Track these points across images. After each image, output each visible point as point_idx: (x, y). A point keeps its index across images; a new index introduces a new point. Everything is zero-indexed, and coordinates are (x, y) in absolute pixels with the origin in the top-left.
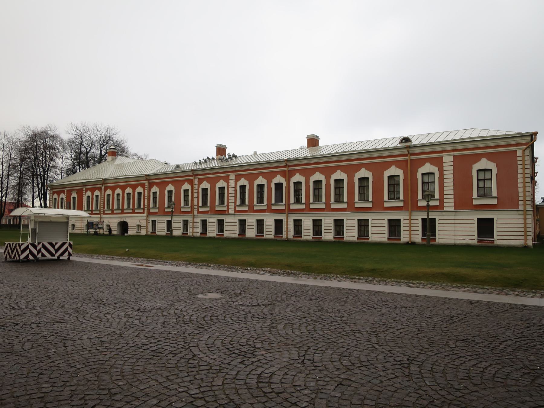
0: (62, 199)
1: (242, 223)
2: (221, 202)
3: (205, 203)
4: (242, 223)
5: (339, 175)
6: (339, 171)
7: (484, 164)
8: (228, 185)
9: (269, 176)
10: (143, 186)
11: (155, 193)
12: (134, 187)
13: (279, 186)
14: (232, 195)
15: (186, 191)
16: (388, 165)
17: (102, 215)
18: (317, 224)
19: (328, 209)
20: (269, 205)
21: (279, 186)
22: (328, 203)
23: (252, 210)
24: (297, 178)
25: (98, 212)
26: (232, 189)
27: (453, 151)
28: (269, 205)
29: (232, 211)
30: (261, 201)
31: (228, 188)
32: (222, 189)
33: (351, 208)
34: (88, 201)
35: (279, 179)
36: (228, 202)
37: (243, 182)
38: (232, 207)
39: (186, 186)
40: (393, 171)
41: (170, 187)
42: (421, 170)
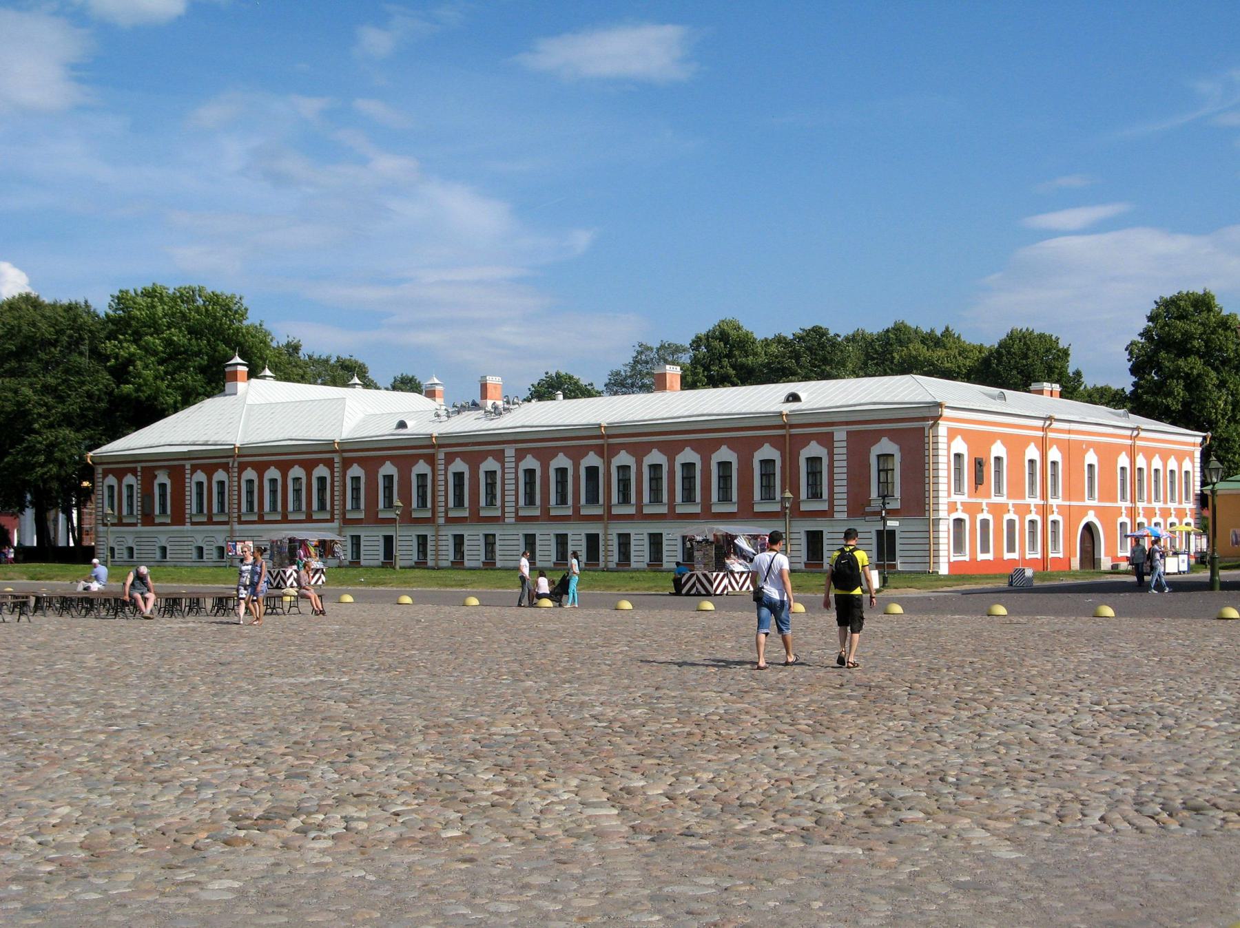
0: (130, 487)
3: (459, 502)
6: (688, 449)
8: (503, 468)
10: (329, 464)
11: (356, 480)
12: (309, 466)
13: (592, 472)
14: (510, 487)
15: (422, 477)
17: (237, 527)
21: (592, 472)
22: (672, 505)
23: (547, 517)
25: (225, 519)
26: (510, 476)
27: (847, 423)
29: (510, 519)
31: (503, 473)
32: (491, 474)
34: (200, 495)
35: (592, 459)
36: (503, 501)
37: (530, 462)
38: (510, 509)
41: (388, 469)
42: (806, 453)
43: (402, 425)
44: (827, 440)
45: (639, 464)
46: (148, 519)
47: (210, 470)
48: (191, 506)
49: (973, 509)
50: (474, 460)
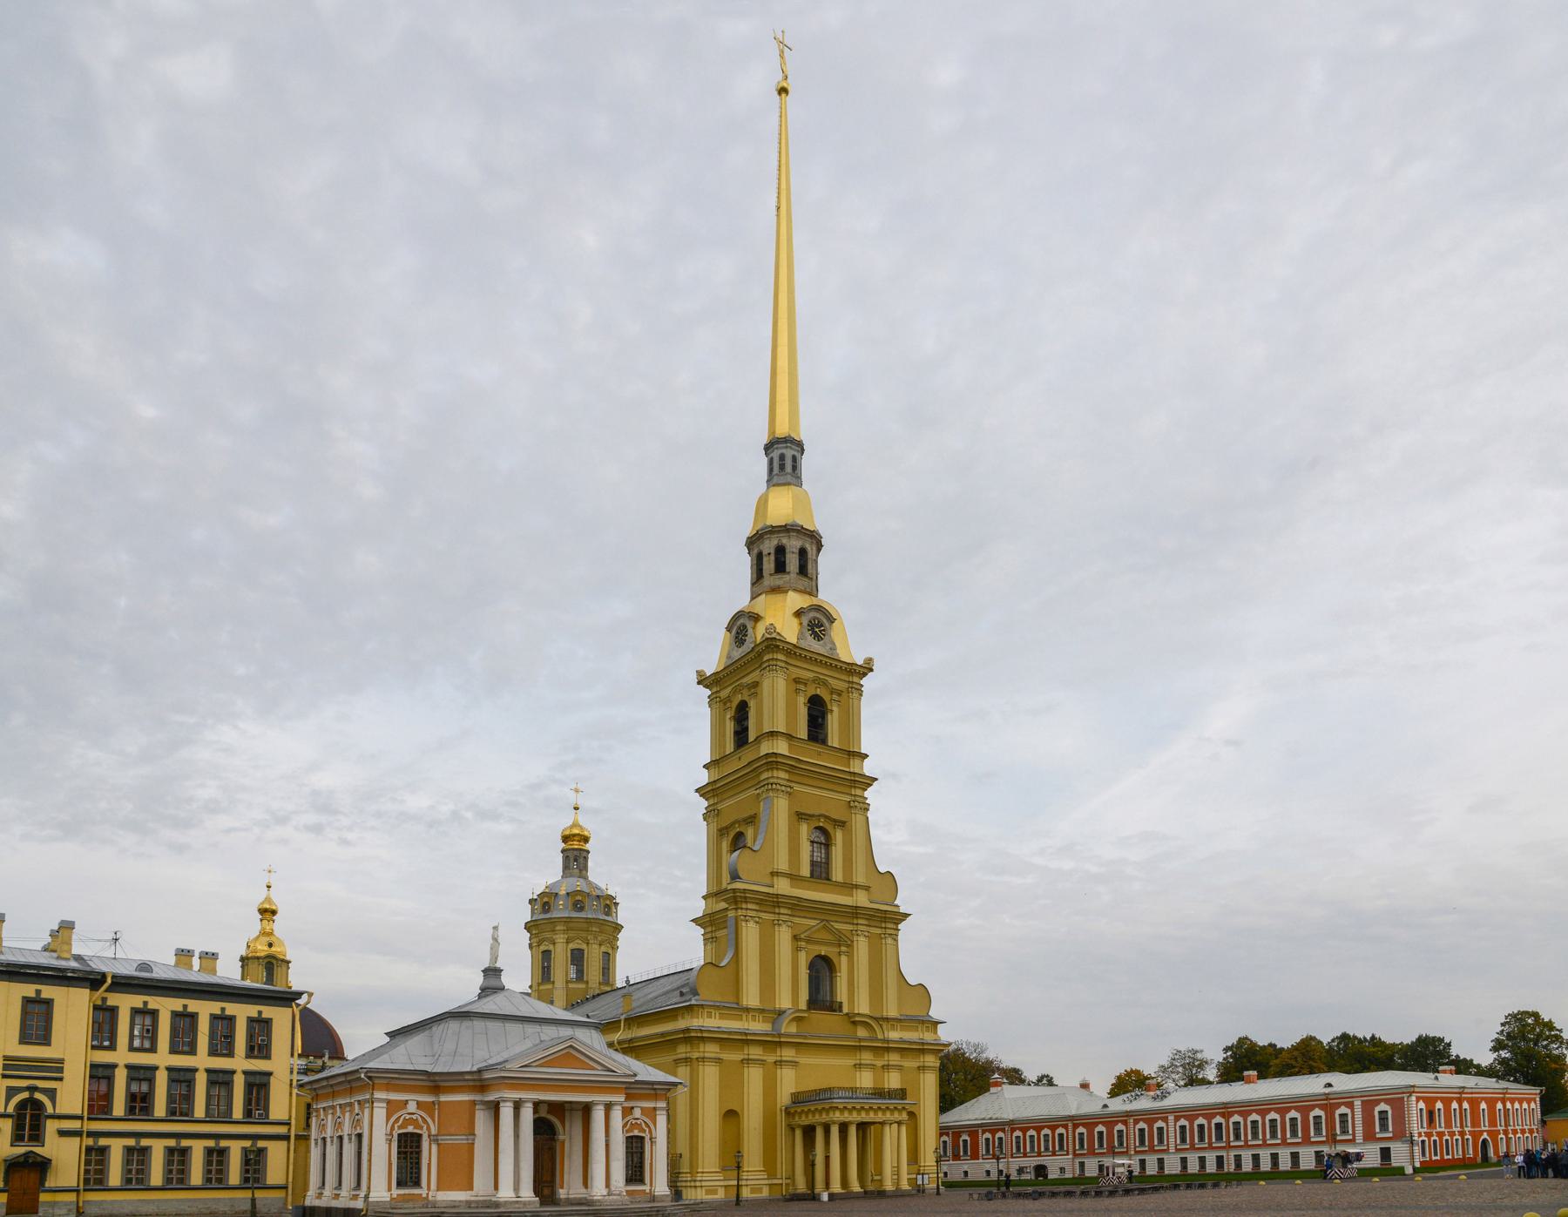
1: (1184, 1160)
2: (1161, 1141)
3: (1142, 1143)
4: (1184, 1160)
5: (1273, 1115)
7: (1383, 1107)
9: (1209, 1117)
10: (1066, 1127)
12: (1053, 1128)
14: (1172, 1134)
15: (1120, 1132)
16: (1313, 1107)
18: (1256, 1158)
19: (1265, 1145)
20: (1210, 1143)
21: (1219, 1126)
23: (1193, 1148)
24: (1236, 1118)
26: (1171, 1129)
28: (1210, 1143)
29: (1172, 1150)
30: (1202, 1139)
32: (1160, 1130)
33: (1284, 1143)
35: (1218, 1119)
37: (1183, 1122)
38: (1172, 1146)
39: (1120, 1127)
40: (1317, 1112)
41: (1101, 1128)
43: (1105, 1106)
44: (1350, 1105)
46: (956, 1157)
47: (993, 1132)
48: (982, 1150)
49: (1429, 1135)
50: (1150, 1122)
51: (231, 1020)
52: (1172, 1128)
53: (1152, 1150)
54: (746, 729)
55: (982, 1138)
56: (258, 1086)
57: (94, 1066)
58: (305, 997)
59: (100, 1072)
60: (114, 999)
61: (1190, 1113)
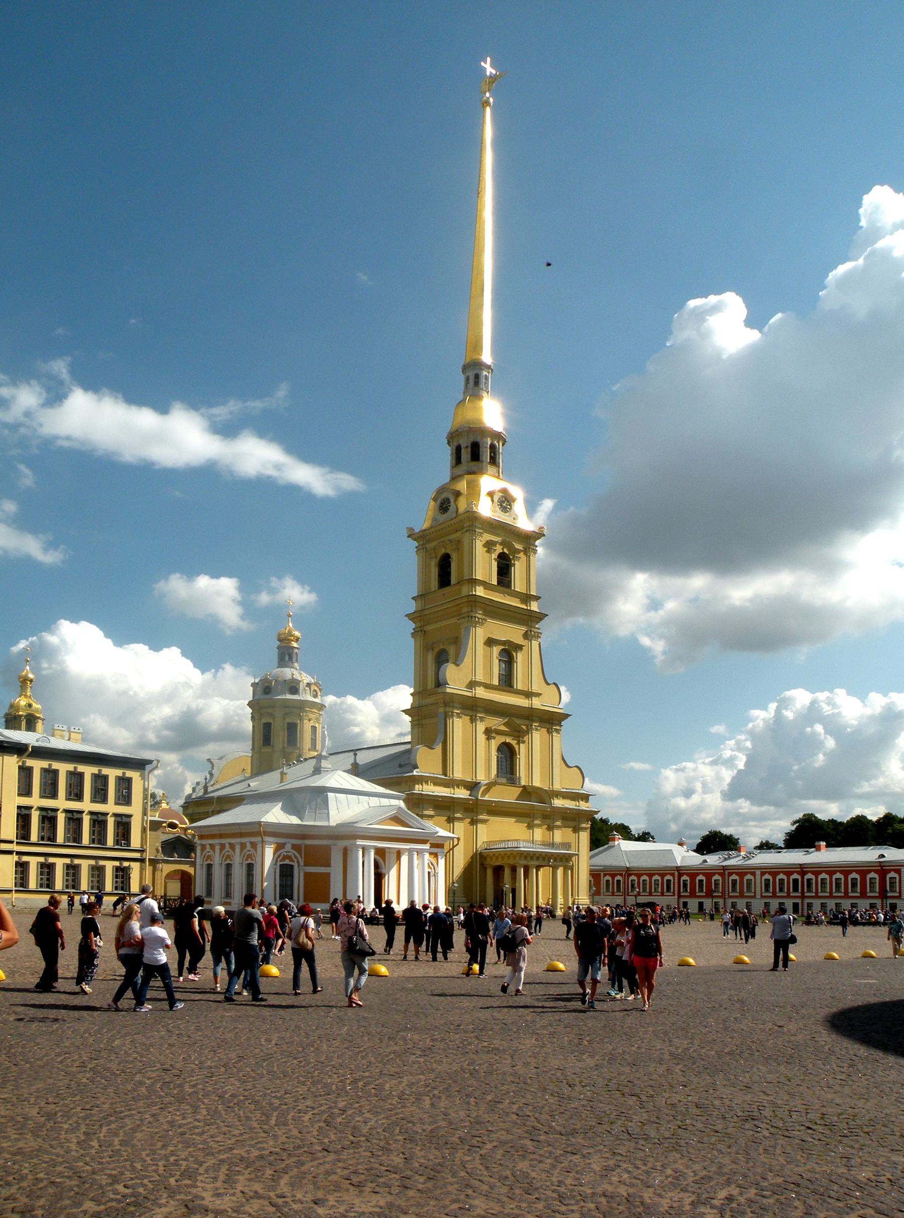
3: (734, 890)
10: (673, 875)
14: (758, 885)
21: (796, 881)
26: (758, 881)
29: (758, 896)
32: (749, 881)
37: (767, 876)
45: (817, 878)
51: (106, 778)
52: (759, 882)
53: (742, 895)
54: (449, 574)
55: (604, 880)
56: (124, 825)
57: (19, 807)
58: (155, 762)
59: (24, 812)
60: (30, 763)
61: (774, 871)
